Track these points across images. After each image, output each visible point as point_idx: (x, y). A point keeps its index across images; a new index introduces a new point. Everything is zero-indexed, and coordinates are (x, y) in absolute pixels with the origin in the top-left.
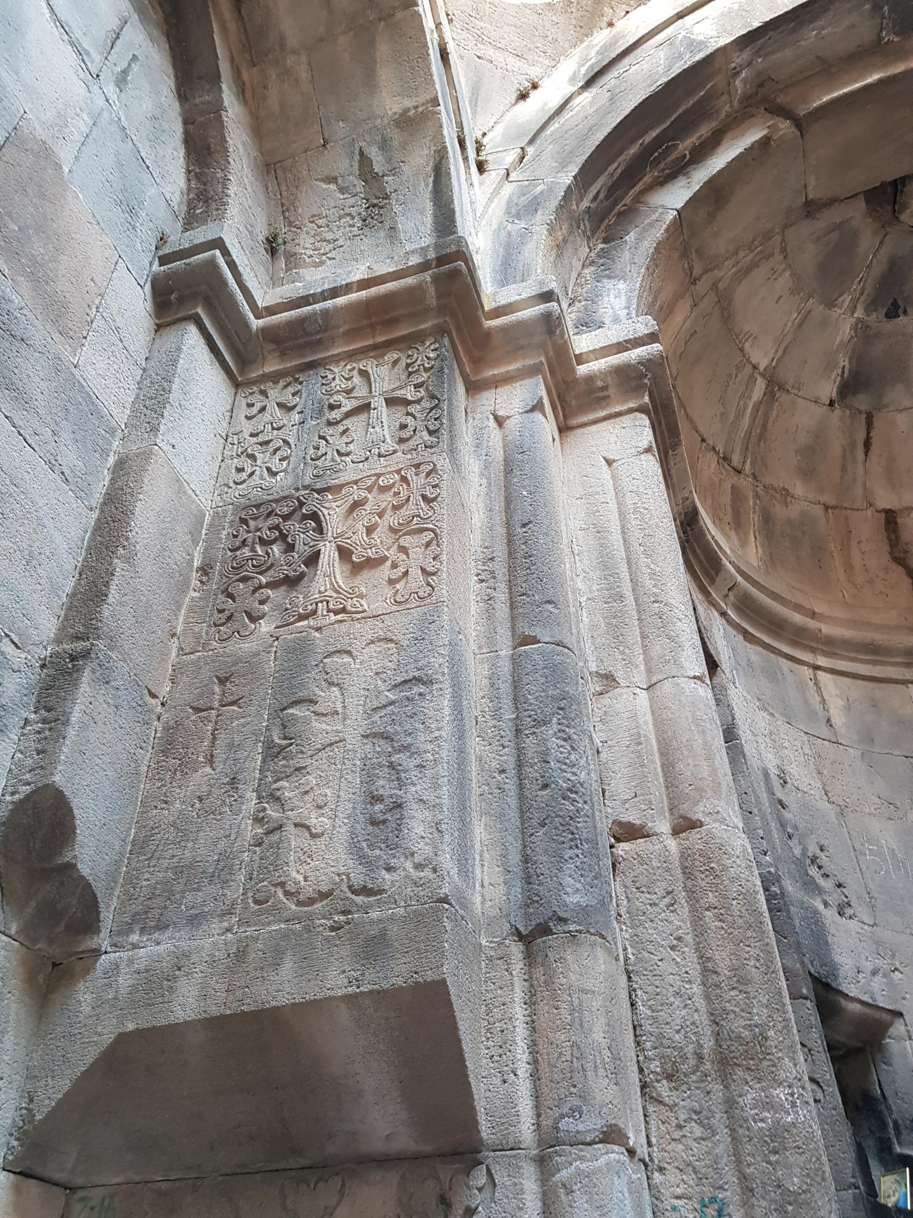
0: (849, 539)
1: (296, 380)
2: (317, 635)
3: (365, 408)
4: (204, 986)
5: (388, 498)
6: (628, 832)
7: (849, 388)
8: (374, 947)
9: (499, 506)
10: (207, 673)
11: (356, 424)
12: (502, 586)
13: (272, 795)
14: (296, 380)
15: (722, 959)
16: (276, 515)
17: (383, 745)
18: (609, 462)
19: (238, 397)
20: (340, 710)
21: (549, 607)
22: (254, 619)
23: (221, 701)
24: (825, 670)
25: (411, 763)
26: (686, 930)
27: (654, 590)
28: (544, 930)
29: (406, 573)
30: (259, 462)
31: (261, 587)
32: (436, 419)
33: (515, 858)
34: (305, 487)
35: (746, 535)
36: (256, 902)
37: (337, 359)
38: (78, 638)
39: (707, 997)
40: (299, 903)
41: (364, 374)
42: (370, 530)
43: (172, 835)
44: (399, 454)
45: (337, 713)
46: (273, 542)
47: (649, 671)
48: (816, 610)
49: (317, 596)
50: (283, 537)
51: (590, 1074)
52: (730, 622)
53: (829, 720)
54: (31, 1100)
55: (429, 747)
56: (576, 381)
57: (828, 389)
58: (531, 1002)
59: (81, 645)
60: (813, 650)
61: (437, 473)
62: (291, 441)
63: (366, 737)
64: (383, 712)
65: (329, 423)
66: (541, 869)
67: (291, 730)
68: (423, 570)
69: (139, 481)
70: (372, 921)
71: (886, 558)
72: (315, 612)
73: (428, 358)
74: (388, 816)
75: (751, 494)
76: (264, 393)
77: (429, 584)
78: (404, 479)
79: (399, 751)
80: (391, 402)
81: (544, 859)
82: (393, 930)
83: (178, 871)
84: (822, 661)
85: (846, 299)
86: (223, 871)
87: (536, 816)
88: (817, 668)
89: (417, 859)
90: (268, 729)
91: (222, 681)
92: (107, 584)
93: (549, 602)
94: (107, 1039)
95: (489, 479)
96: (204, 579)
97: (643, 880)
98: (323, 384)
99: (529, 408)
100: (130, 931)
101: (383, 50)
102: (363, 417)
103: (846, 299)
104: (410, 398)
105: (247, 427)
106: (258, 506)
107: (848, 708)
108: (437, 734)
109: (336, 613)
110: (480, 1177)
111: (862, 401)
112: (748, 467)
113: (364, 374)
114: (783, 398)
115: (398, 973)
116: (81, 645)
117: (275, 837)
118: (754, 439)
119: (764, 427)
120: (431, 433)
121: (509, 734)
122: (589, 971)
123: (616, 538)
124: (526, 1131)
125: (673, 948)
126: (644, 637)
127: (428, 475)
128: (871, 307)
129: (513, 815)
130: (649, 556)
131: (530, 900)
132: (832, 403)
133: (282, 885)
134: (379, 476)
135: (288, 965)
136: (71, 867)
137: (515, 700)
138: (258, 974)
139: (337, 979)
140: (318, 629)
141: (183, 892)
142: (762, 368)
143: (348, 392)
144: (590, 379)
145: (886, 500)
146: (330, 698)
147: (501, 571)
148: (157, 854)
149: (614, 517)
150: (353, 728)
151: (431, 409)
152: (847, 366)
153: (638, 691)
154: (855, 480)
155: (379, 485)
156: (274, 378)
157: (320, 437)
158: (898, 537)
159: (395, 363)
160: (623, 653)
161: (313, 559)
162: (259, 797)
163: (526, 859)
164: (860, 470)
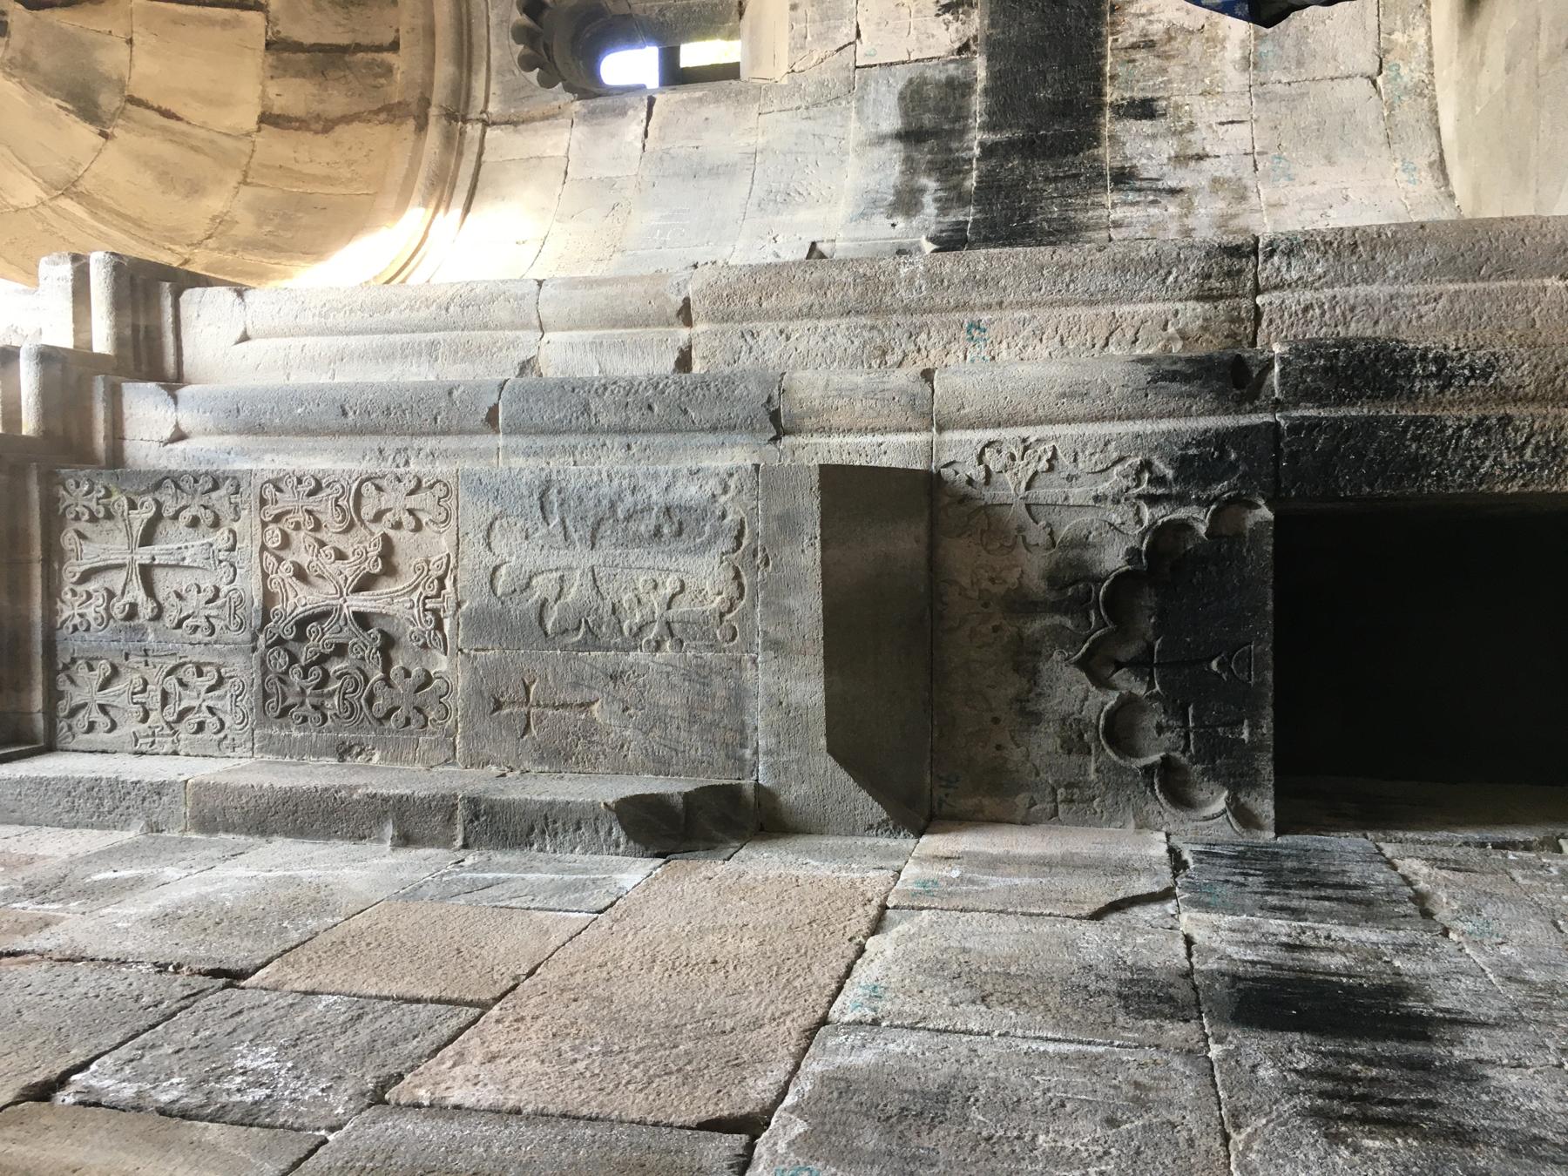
0: (290, 170)
1: (66, 667)
2: (464, 607)
3: (146, 572)
4: (798, 677)
5: (301, 539)
6: (684, 362)
8: (787, 524)
9: (308, 442)
10: (484, 726)
11: (166, 584)
12: (418, 442)
13: (636, 635)
14: (66, 667)
15: (801, 299)
16: (286, 673)
17: (606, 528)
18: (245, 338)
19: (73, 745)
20: (560, 573)
21: (456, 394)
22: (428, 679)
23: (521, 704)
25: (629, 500)
26: (776, 326)
27: (434, 307)
28: (775, 417)
29: (411, 512)
30: (195, 703)
31: (387, 680)
32: (196, 481)
33: (711, 439)
34: (255, 638)
35: (274, 271)
36: (733, 638)
37: (50, 612)
38: (450, 820)
39: (829, 317)
40: (741, 596)
41: (86, 577)
42: (341, 556)
43: (657, 732)
44: (236, 526)
45: (562, 577)
46: (326, 673)
47: (525, 326)
49: (415, 611)
50: (322, 659)
51: (887, 386)
54: (871, 827)
55: (616, 482)
56: (119, 356)
58: (827, 431)
59: (460, 814)
61: (280, 479)
62: (172, 662)
63: (593, 545)
64: (571, 529)
65: (157, 617)
66: (724, 415)
67: (571, 625)
68: (412, 493)
69: (240, 791)
70: (766, 528)
72: (435, 612)
73: (88, 493)
74: (676, 520)
75: (216, 254)
76: (74, 712)
77: (431, 487)
78: (277, 519)
79: (615, 512)
80: (147, 538)
81: (716, 411)
82: (776, 510)
83: (693, 719)
86: (699, 676)
87: (677, 416)
89: (718, 491)
90: (564, 648)
91: (498, 706)
92: (386, 800)
93: (450, 393)
94: (830, 762)
95: (266, 451)
96: (357, 749)
97: (728, 357)
98: (88, 630)
99: (172, 401)
100: (741, 759)
102: (159, 575)
104: (150, 514)
105: (130, 726)
106: (266, 696)
108: (604, 475)
109: (442, 587)
110: (948, 473)
111: (108, 101)
113: (86, 577)
114: (86, 185)
115: (810, 504)
116: (460, 814)
117: (676, 627)
120: (216, 487)
121: (592, 440)
122: (810, 385)
123: (354, 342)
124: (921, 438)
125: (788, 338)
126: (486, 327)
127: (280, 490)
129: (676, 438)
130: (388, 310)
131: (749, 427)
132: (104, 135)
133: (722, 615)
134: (263, 548)
135: (792, 602)
136: (686, 796)
137: (556, 432)
138: (794, 628)
139: (807, 556)
140: (459, 605)
141: (713, 711)
143: (111, 595)
144: (119, 341)
145: (247, 118)
146: (543, 586)
147: (399, 442)
148: (673, 745)
149: (325, 341)
150: (581, 558)
151: (177, 486)
152: (57, 101)
153: (545, 339)
154: (212, 142)
155: (279, 548)
156: (53, 695)
157: (179, 625)
158: (297, 119)
159: (81, 536)
160: (500, 349)
161: (363, 619)
162: (635, 649)
163: (714, 429)
164: (202, 133)
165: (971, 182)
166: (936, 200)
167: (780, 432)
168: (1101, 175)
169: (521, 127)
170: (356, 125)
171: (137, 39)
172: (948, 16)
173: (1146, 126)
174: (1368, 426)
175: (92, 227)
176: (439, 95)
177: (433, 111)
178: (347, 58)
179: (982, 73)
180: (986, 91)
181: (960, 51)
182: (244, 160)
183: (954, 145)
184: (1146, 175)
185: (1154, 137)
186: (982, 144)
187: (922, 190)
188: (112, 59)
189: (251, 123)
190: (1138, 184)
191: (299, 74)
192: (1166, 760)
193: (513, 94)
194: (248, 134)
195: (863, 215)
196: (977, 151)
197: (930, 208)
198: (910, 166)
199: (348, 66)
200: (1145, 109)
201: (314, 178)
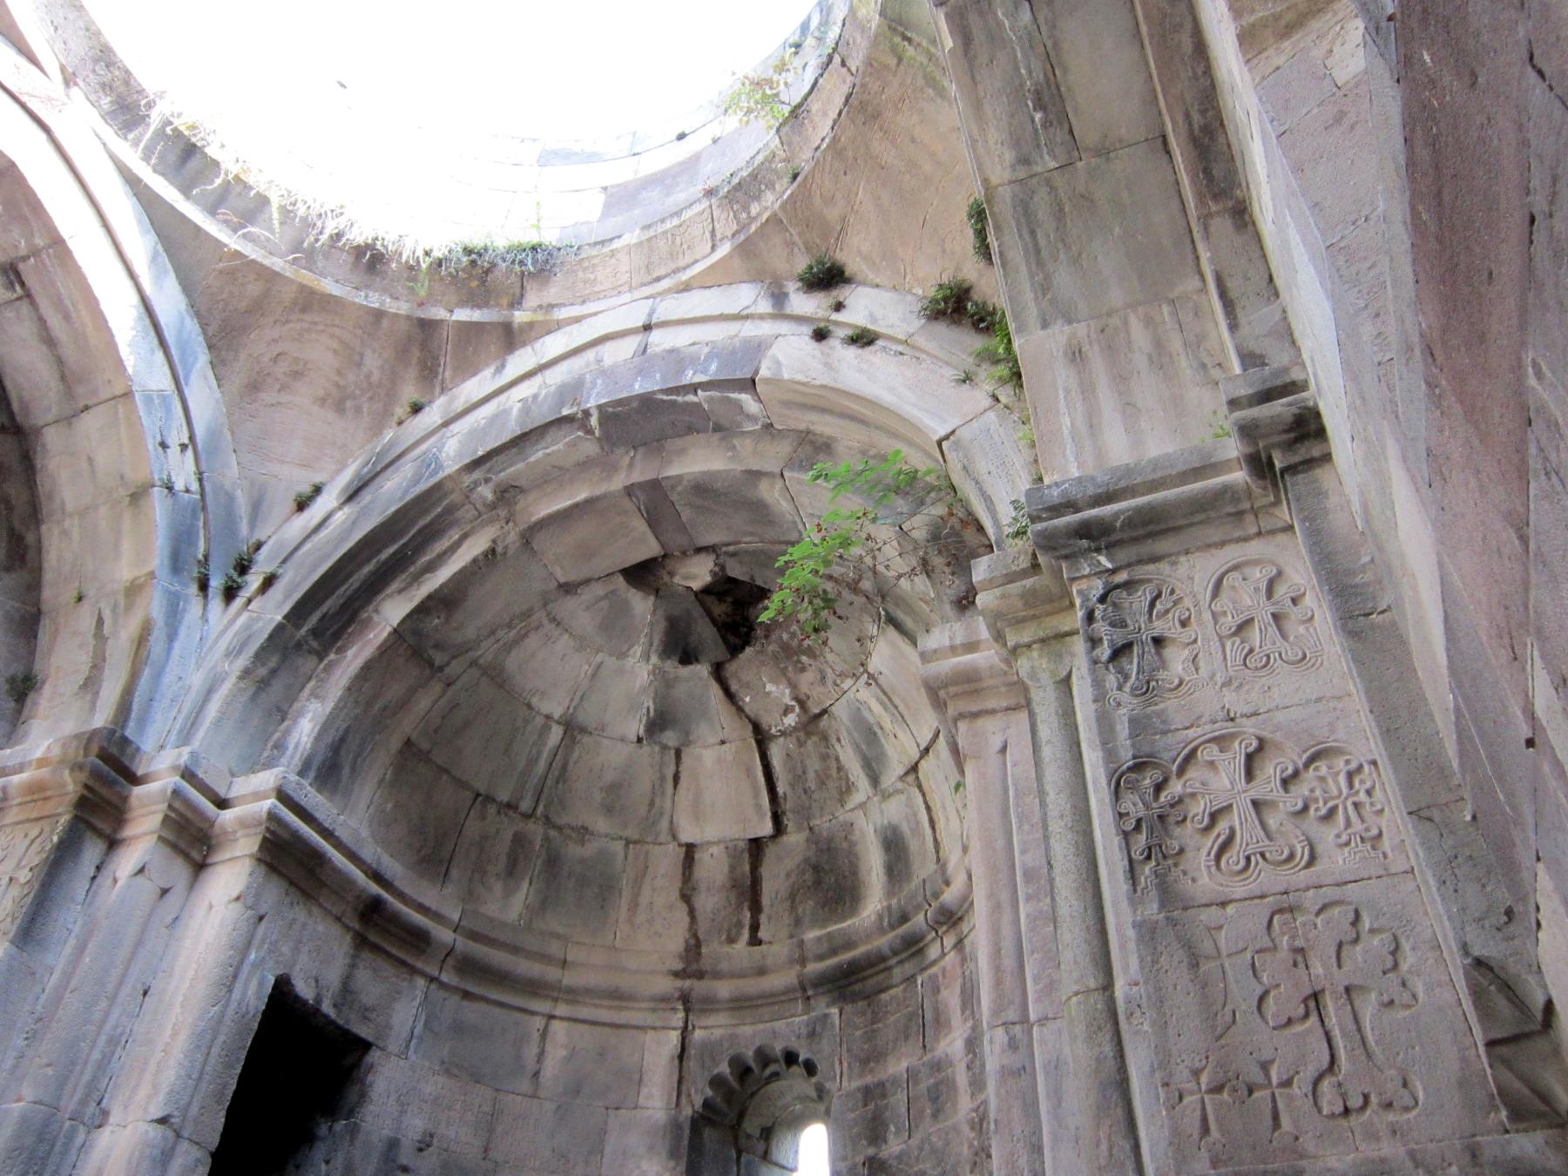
0: (644, 876)
7: (658, 723)
24: (562, 1019)
48: (569, 958)
52: (443, 986)
53: (536, 1074)
57: (635, 727)
60: (556, 1000)
71: (677, 894)
84: (562, 1010)
85: (638, 650)
88: (551, 1017)
101: (127, 524)
103: (638, 650)
107: (569, 1058)
111: (670, 738)
112: (540, 809)
118: (549, 783)
119: (564, 767)
128: (666, 653)
132: (639, 740)
142: (556, 716)
154: (662, 814)
169: (676, 1062)
170: (687, 919)
171: (726, 747)
175: (539, 753)
176: (700, 987)
177: (688, 983)
178: (746, 905)
182: (649, 839)
188: (706, 733)
189: (686, 836)
191: (732, 868)
193: (710, 1050)
194: (674, 837)
199: (739, 907)
201: (636, 895)
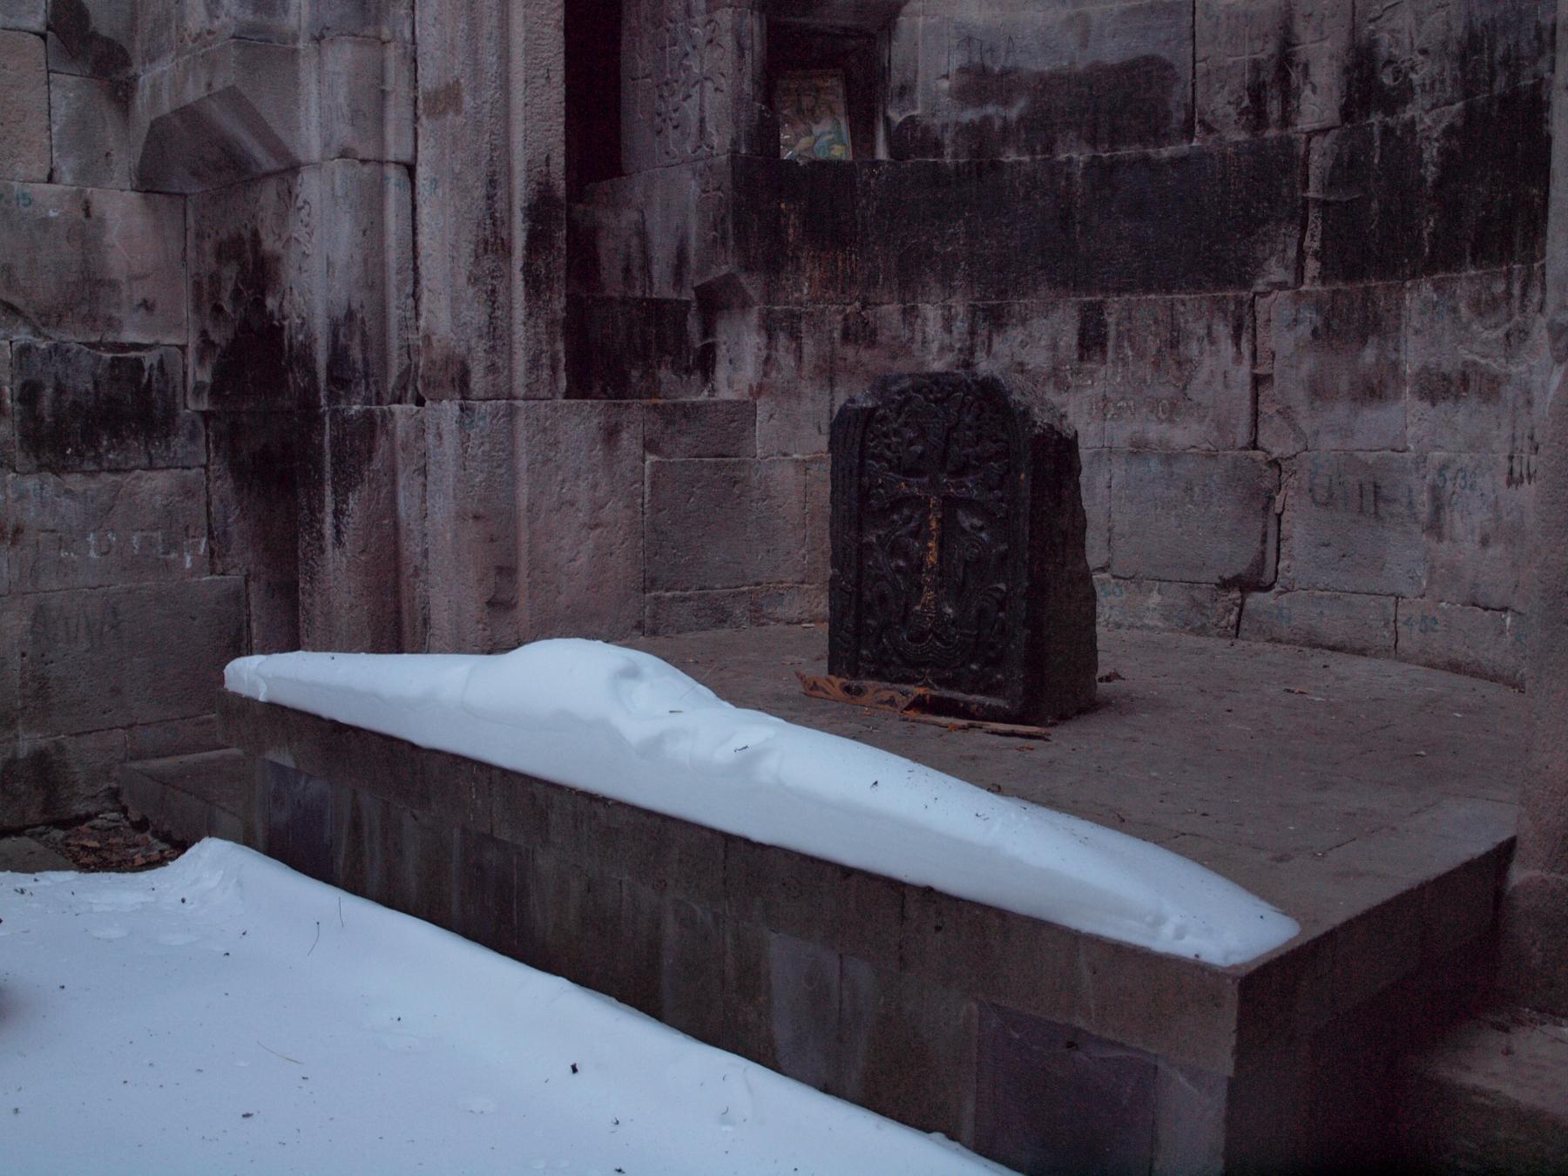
165: (1011, 157)
166: (987, 119)
167: (318, 39)
168: (1002, 294)
172: (1246, 102)
173: (1069, 338)
174: (320, 470)
179: (1166, 152)
180: (1146, 159)
181: (1202, 122)
183: (1072, 135)
184: (996, 340)
185: (1054, 347)
186: (1070, 160)
187: (1006, 103)
190: (983, 330)
192: (213, 344)
195: (969, 39)
196: (1062, 157)
197: (970, 115)
198: (1046, 84)
200: (1092, 341)
